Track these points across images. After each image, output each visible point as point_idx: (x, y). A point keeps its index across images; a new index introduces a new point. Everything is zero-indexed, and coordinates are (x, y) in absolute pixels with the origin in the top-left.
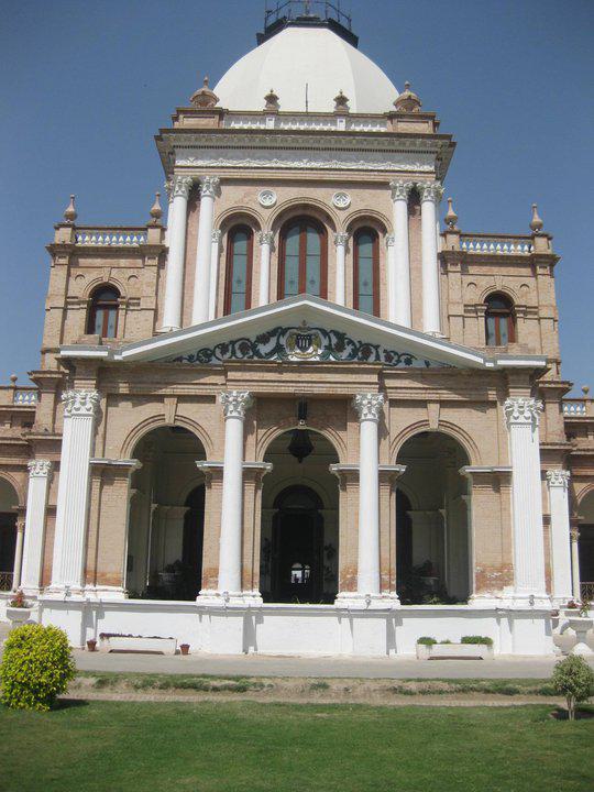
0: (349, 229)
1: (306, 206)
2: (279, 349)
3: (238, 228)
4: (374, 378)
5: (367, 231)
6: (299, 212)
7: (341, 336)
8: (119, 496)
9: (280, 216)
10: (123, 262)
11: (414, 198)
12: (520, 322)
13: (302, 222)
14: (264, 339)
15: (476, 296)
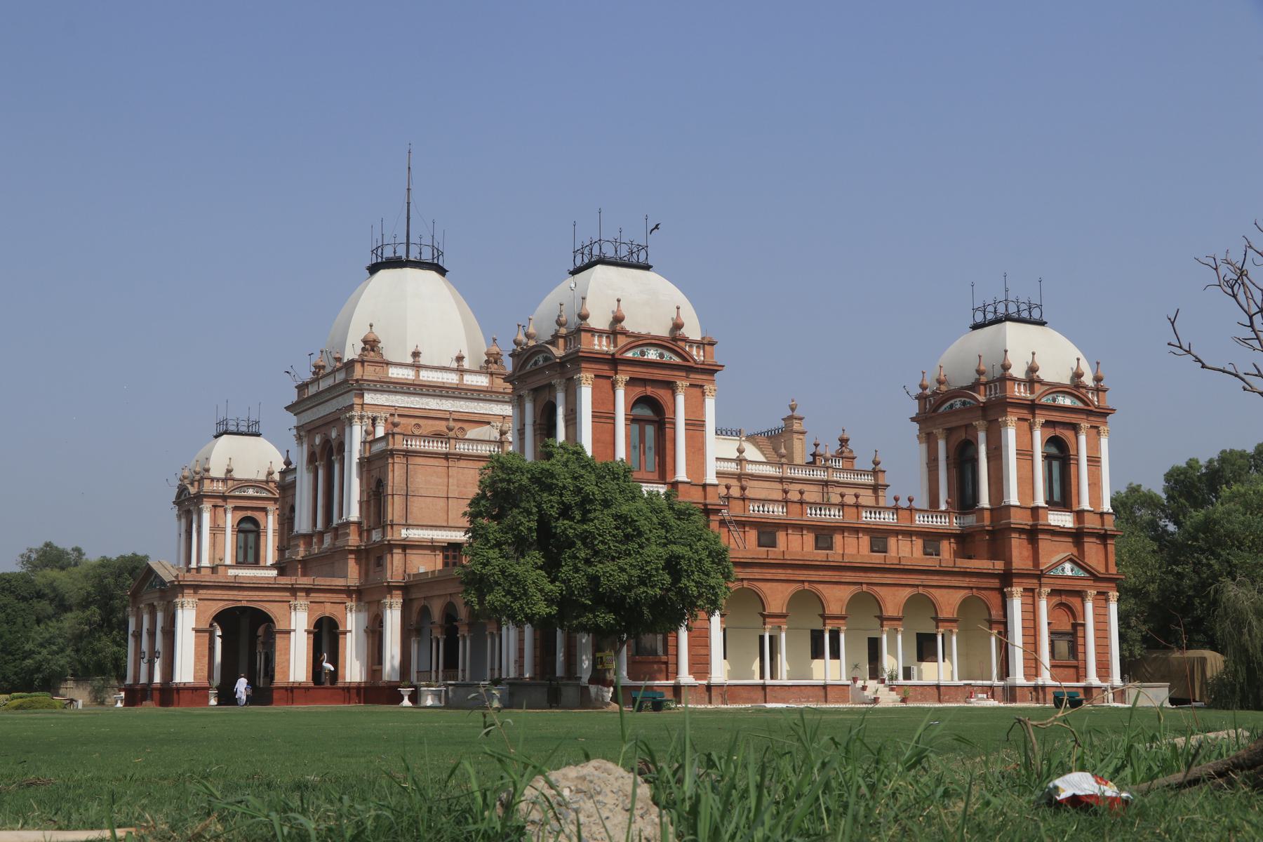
4: (158, 595)
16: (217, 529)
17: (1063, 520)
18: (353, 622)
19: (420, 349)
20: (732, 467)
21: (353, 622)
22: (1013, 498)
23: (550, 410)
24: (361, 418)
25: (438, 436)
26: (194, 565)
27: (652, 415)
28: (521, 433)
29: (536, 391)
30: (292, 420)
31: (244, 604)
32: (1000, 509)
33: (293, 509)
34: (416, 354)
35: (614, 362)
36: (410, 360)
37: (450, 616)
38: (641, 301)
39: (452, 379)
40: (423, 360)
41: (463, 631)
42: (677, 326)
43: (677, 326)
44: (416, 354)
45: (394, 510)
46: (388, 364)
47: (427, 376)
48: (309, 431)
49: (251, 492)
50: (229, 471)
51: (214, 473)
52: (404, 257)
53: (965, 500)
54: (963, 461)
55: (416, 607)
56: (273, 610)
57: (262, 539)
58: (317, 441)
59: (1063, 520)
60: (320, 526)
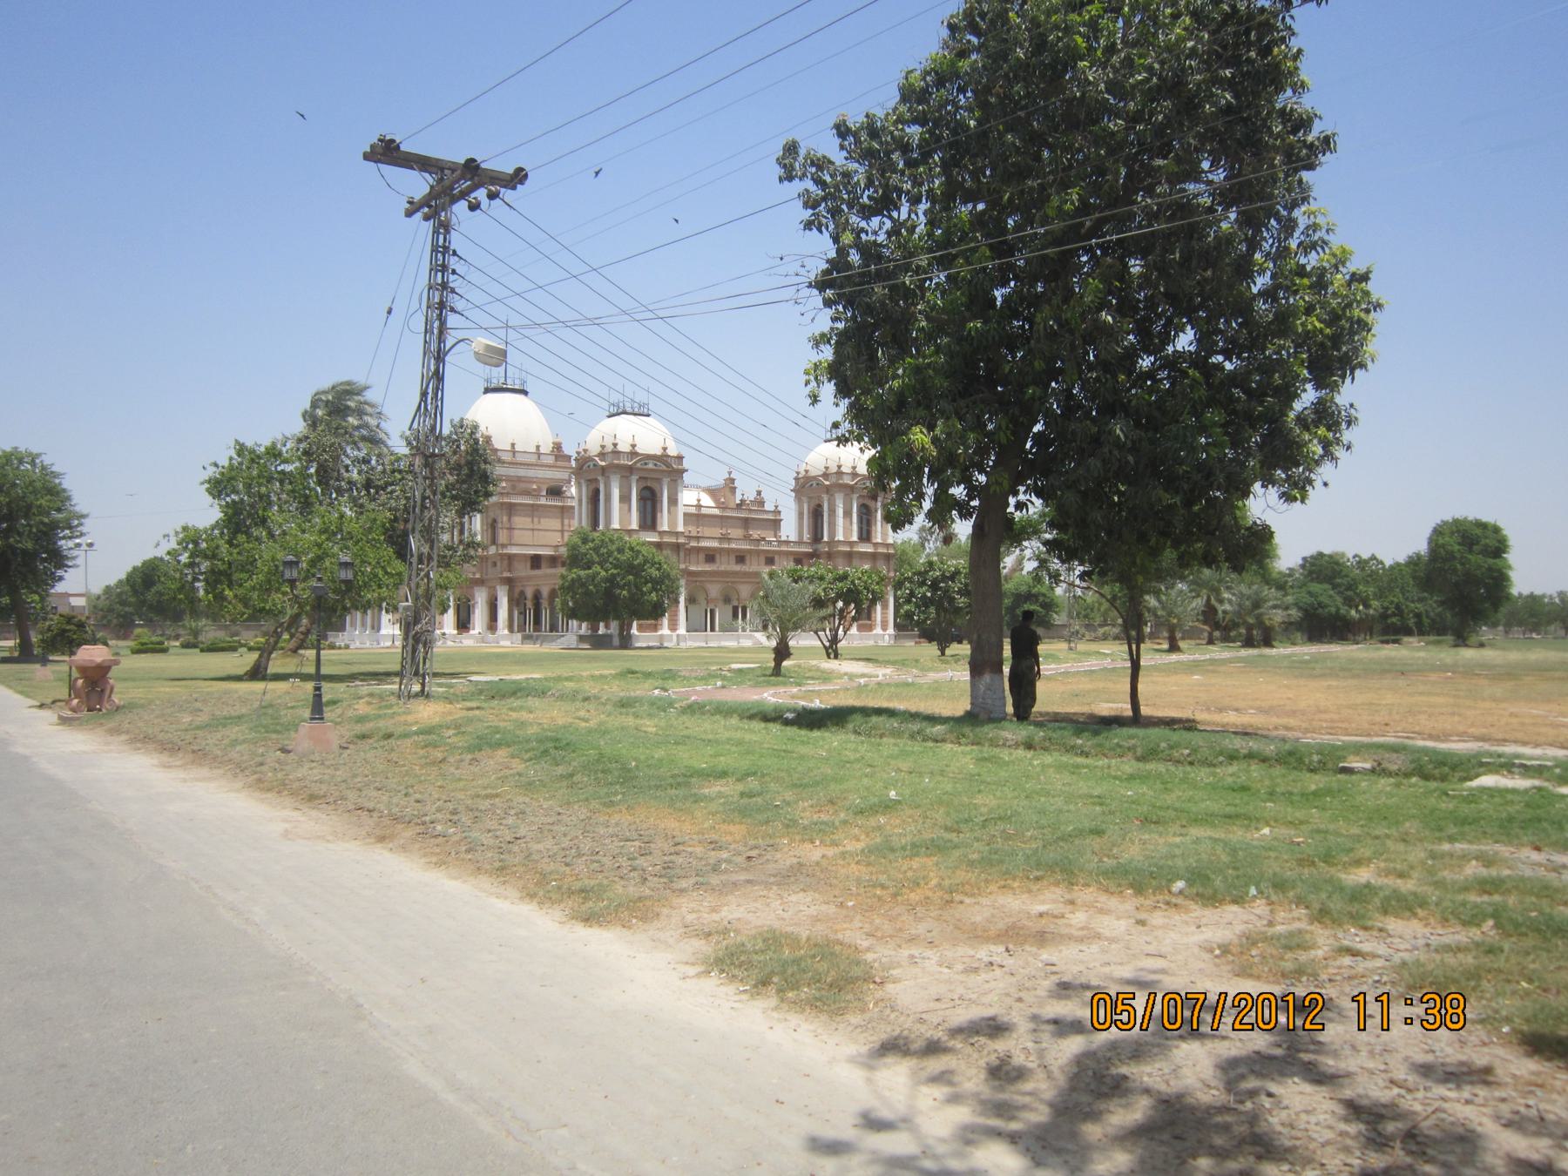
17: (866, 548)
20: (693, 510)
22: (840, 537)
23: (597, 492)
25: (527, 493)
27: (650, 503)
28: (580, 501)
29: (590, 481)
32: (832, 542)
35: (631, 469)
37: (537, 597)
38: (645, 436)
41: (545, 603)
42: (665, 449)
43: (665, 449)
45: (502, 537)
47: (519, 458)
53: (817, 537)
54: (817, 514)
55: (517, 590)
59: (866, 548)
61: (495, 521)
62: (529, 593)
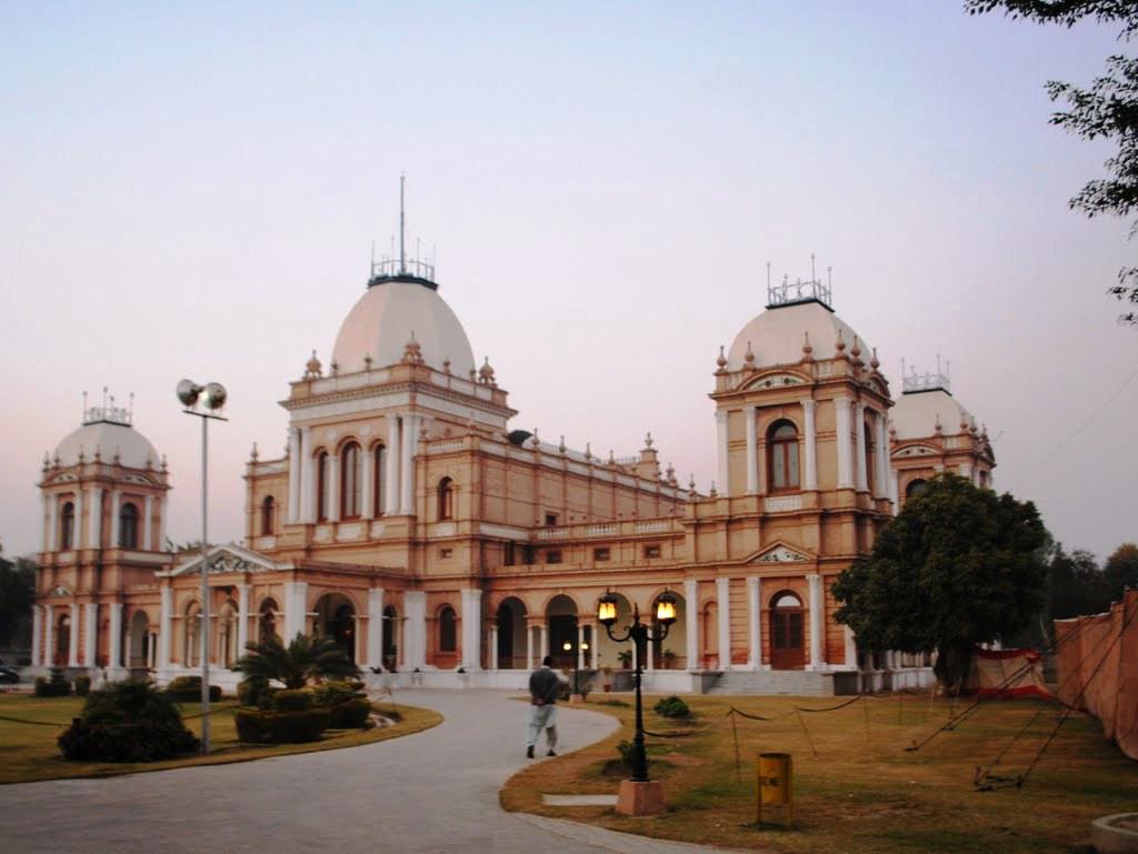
0: (371, 447)
1: (352, 437)
2: (222, 568)
3: (321, 455)
4: (243, 578)
5: (378, 448)
6: (347, 441)
7: (239, 558)
8: (180, 628)
9: (340, 444)
10: (276, 481)
11: (400, 421)
12: (454, 496)
13: (348, 445)
14: (217, 562)
15: (434, 482)
16: (105, 514)
18: (416, 609)
19: (451, 360)
21: (416, 609)
24: (414, 417)
26: (76, 545)
30: (285, 416)
31: (338, 591)
33: (269, 500)
34: (447, 364)
36: (440, 368)
39: (467, 389)
40: (453, 370)
44: (447, 364)
46: (432, 370)
48: (312, 427)
49: (135, 479)
50: (117, 458)
51: (104, 459)
52: (415, 275)
56: (356, 597)
57: (140, 524)
58: (331, 438)
60: (332, 513)
61: (446, 480)
62: (536, 603)
